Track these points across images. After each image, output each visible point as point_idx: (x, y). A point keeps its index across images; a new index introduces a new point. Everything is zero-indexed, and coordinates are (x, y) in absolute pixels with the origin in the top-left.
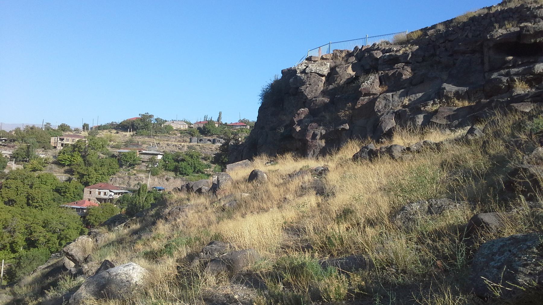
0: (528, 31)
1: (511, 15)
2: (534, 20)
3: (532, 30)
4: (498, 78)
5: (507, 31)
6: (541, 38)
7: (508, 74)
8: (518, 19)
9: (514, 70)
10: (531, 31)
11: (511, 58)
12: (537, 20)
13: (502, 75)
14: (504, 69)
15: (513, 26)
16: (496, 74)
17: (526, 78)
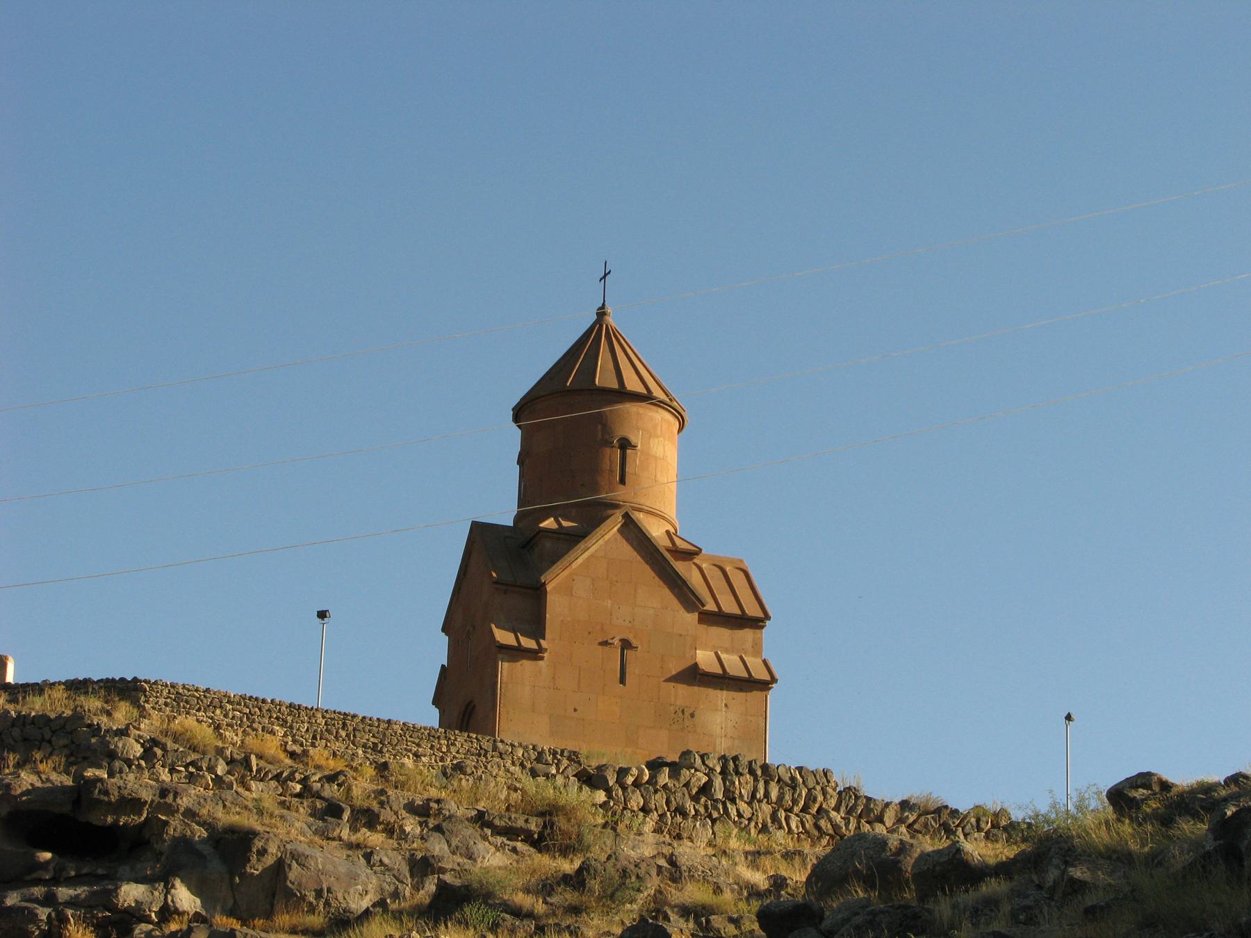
0: (107, 793)
1: (47, 735)
2: (109, 765)
3: (116, 793)
4: (26, 908)
5: (43, 782)
6: (129, 816)
7: (49, 900)
8: (66, 751)
9: (64, 893)
10: (113, 795)
11: (48, 855)
12: (117, 764)
13: (36, 901)
14: (38, 882)
15: (54, 769)
16: (15, 895)
17: (93, 916)
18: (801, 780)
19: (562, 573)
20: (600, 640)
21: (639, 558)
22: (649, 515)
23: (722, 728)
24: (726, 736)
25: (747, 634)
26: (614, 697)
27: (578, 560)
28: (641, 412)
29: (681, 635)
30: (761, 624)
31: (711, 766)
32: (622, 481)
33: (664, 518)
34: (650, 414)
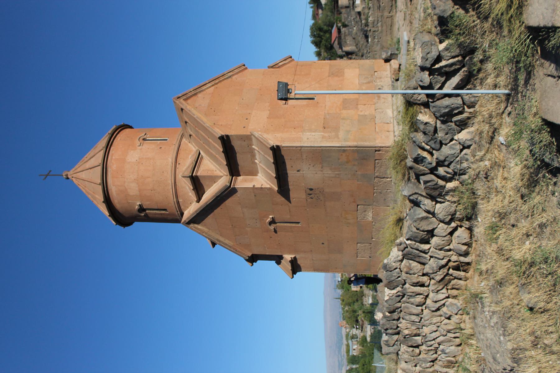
18: (399, 289)
19: (239, 250)
20: (274, 233)
21: (211, 215)
22: (178, 196)
23: (316, 173)
24: (322, 171)
25: (236, 144)
26: (309, 227)
27: (227, 243)
28: (117, 201)
29: (255, 196)
30: (225, 138)
31: (394, 342)
32: (165, 210)
33: (175, 183)
34: (115, 195)
